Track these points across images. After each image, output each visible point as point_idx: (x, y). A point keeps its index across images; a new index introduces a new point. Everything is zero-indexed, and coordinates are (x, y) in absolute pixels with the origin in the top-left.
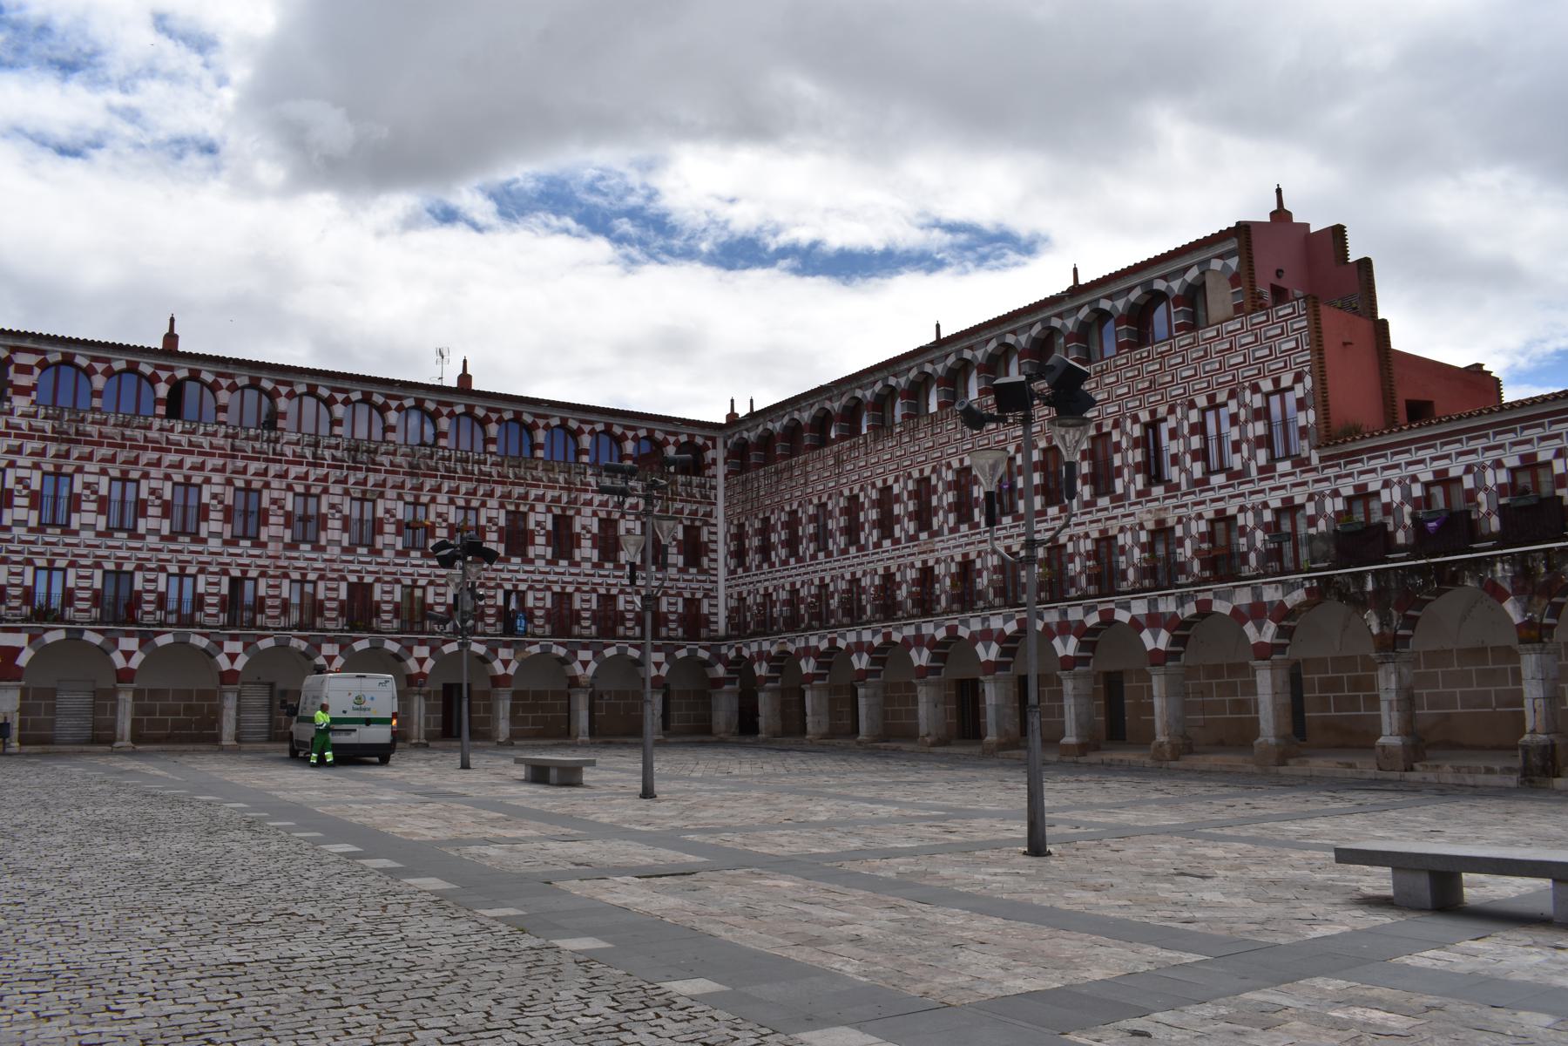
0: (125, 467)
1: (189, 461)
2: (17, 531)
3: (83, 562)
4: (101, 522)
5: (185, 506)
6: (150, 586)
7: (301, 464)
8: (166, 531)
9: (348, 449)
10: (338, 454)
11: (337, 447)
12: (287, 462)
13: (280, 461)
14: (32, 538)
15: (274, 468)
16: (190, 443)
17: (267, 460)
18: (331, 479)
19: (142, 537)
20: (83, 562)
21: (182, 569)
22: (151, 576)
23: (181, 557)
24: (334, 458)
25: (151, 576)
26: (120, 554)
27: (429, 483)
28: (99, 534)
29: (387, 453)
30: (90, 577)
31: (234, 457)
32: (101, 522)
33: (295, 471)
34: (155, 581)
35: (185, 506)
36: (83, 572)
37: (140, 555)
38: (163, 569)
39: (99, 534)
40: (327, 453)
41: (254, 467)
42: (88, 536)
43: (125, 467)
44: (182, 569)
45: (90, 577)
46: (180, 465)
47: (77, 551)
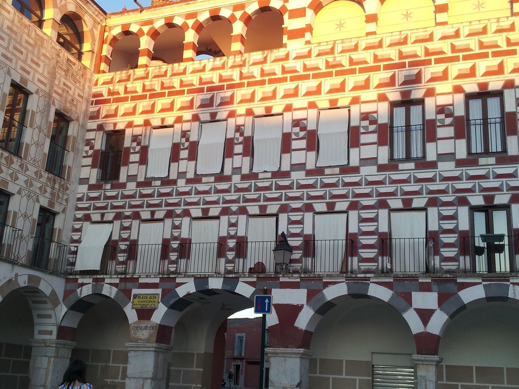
0: (406, 88)
3: (365, 202)
4: (383, 155)
5: (485, 121)
6: (448, 225)
8: (462, 154)
14: (311, 182)
16: (481, 45)
19: (433, 165)
20: (365, 202)
21: (489, 199)
22: (448, 211)
23: (486, 184)
25: (448, 211)
26: (407, 188)
28: (381, 168)
30: (375, 220)
32: (383, 155)
34: (454, 217)
35: (485, 121)
36: (367, 214)
37: (433, 187)
38: (463, 201)
39: (381, 168)
42: (369, 172)
43: (406, 88)
44: (489, 199)
45: (375, 220)
46: (472, 73)
47: (358, 190)
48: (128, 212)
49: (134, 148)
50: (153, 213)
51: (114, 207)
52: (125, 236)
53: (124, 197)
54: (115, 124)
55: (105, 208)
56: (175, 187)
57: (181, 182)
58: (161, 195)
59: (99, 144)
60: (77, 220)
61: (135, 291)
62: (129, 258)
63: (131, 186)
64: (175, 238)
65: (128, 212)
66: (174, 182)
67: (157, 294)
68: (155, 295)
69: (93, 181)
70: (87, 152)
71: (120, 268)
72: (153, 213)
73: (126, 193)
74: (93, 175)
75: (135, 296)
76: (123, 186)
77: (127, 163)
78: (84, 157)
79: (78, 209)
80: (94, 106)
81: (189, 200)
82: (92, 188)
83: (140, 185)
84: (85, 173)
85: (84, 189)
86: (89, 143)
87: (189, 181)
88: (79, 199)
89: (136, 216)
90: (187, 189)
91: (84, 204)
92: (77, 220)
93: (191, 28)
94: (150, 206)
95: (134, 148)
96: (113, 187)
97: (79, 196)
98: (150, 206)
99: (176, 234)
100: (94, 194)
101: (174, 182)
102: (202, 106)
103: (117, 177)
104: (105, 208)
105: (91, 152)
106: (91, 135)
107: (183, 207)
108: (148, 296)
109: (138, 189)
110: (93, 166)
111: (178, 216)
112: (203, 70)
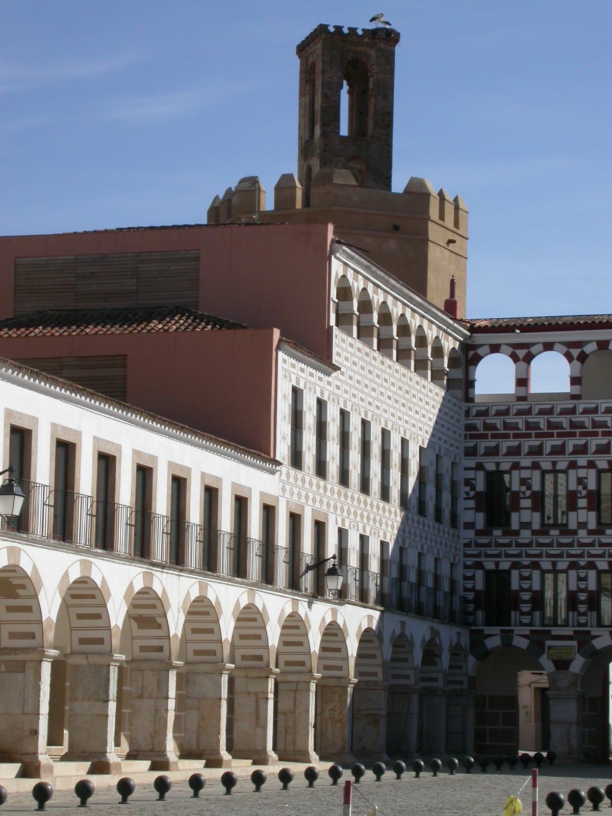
2: (582, 533)
48: (526, 561)
49: (524, 493)
50: (554, 564)
51: (508, 556)
52: (526, 586)
53: (519, 545)
54: (498, 464)
55: (499, 556)
56: (576, 537)
57: (582, 533)
58: (561, 545)
59: (480, 486)
60: (466, 567)
61: (548, 643)
62: (534, 609)
63: (526, 535)
64: (582, 591)
65: (526, 561)
66: (574, 532)
67: (574, 646)
68: (570, 647)
69: (480, 525)
70: (467, 493)
71: (526, 620)
72: (554, 564)
73: (521, 541)
74: (480, 519)
75: (550, 648)
76: (516, 533)
77: (517, 508)
78: (465, 499)
79: (466, 555)
80: (468, 440)
81: (593, 552)
82: (479, 533)
83: (535, 533)
84: (467, 516)
85: (470, 534)
86: (468, 482)
87: (590, 532)
88: (467, 545)
89: (536, 566)
90: (589, 540)
91: (473, 551)
92: (466, 567)
93: (577, 359)
94: (549, 556)
95: (524, 493)
96: (505, 534)
97: (467, 541)
98: (549, 556)
99: (582, 586)
100: (484, 540)
101: (574, 532)
102: (597, 452)
103: (508, 522)
104: (499, 556)
105: (472, 493)
106: (470, 474)
107: (587, 559)
108: (564, 648)
109: (534, 537)
110: (478, 509)
111: (582, 568)
112: (595, 411)
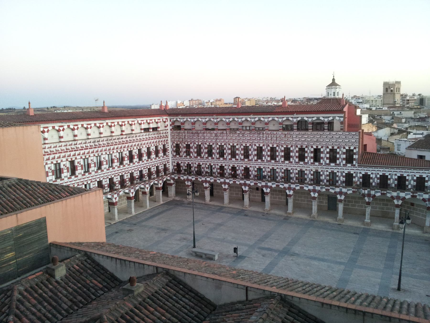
1: (57, 156)
7: (83, 149)
9: (93, 142)
10: (91, 144)
11: (90, 142)
12: (80, 150)
13: (78, 150)
15: (77, 152)
16: (56, 151)
17: (75, 151)
18: (90, 152)
24: (90, 146)
27: (112, 147)
29: (102, 141)
31: (67, 152)
33: (82, 152)
40: (89, 145)
41: (72, 153)
